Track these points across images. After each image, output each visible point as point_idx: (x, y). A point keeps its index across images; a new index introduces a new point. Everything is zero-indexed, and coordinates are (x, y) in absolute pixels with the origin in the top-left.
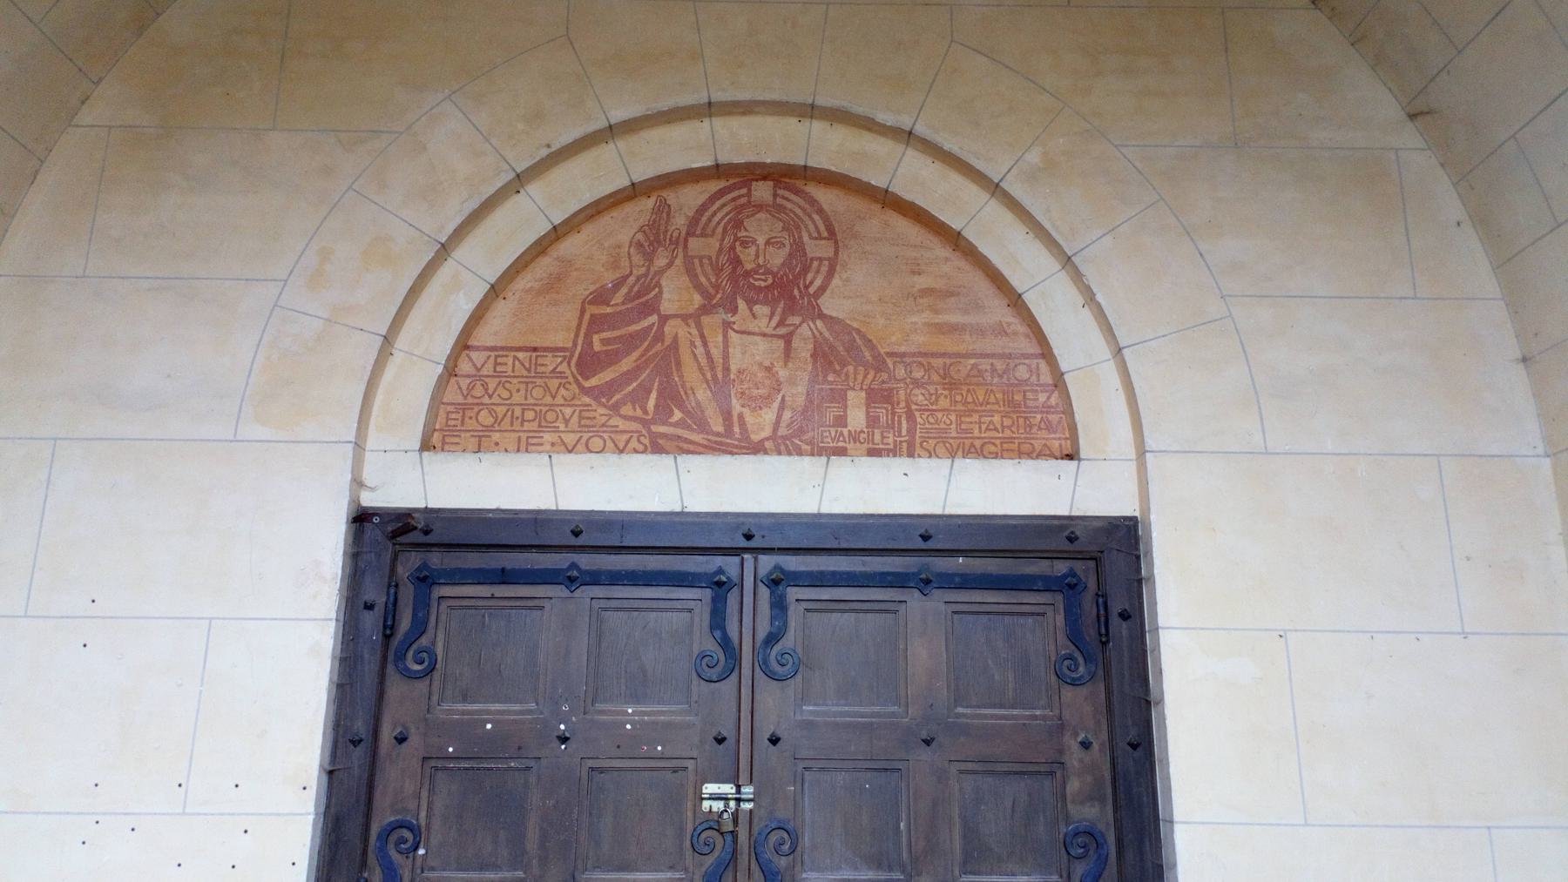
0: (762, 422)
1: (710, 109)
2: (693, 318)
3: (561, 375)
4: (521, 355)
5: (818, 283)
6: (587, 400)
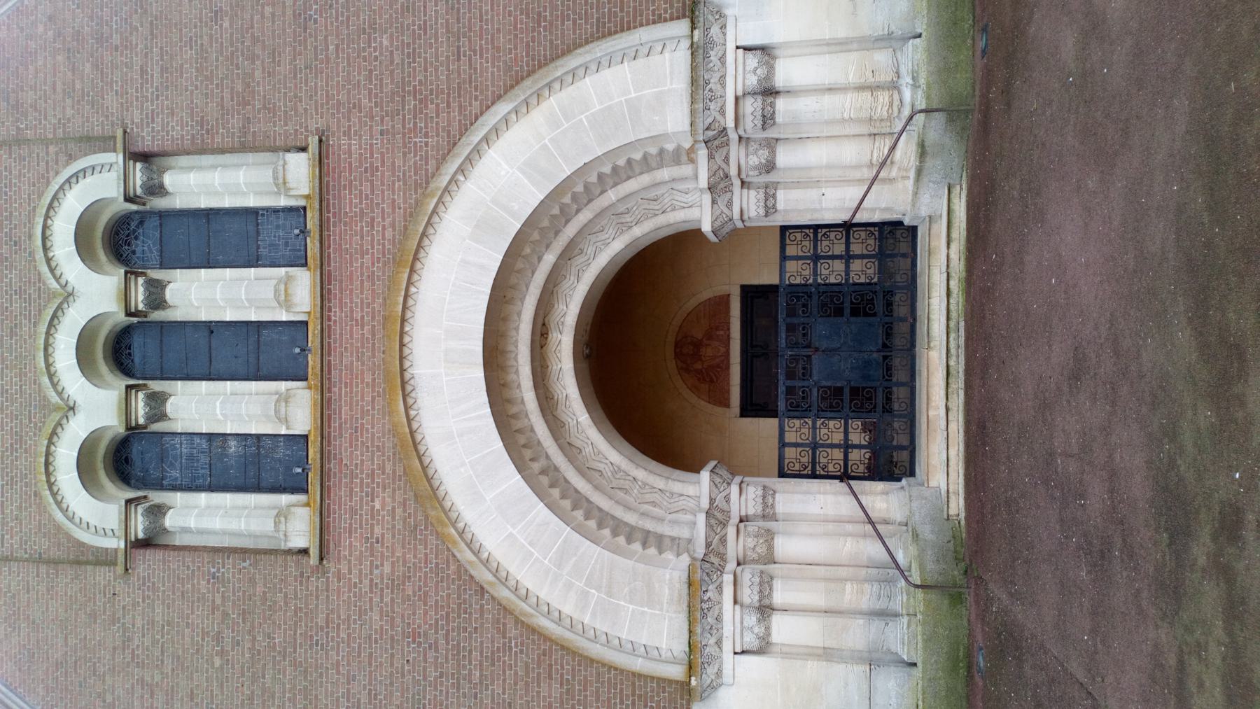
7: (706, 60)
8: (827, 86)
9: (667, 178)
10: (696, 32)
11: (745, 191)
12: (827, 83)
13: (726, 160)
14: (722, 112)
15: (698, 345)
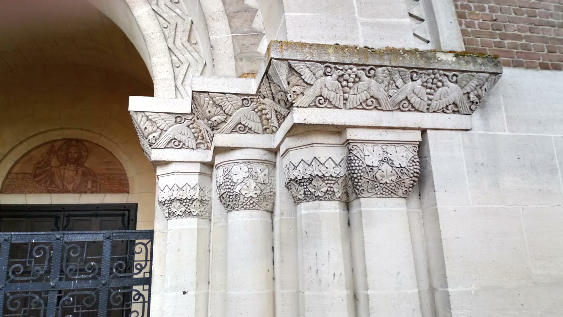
0: (70, 187)
1: (61, 129)
2: (57, 167)
3: (29, 178)
4: (22, 174)
5: (84, 160)
6: (34, 183)
7: (408, 72)
8: (361, 293)
9: (214, 37)
10: (451, 58)
11: (197, 168)
12: (369, 292)
13: (240, 128)
15: (78, 162)
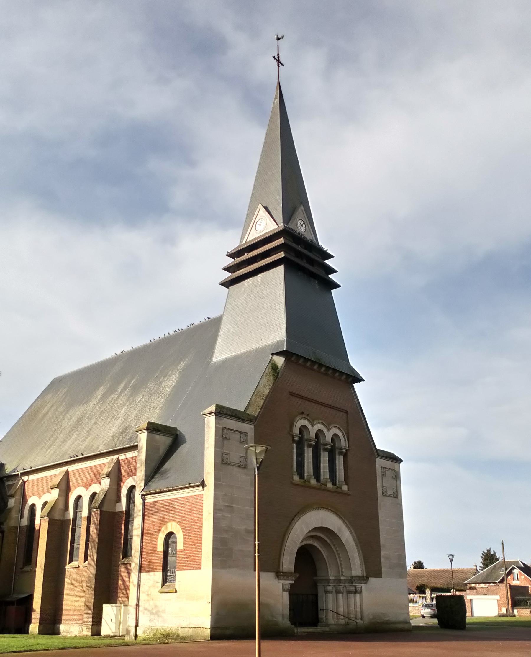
14: (355, 583)
